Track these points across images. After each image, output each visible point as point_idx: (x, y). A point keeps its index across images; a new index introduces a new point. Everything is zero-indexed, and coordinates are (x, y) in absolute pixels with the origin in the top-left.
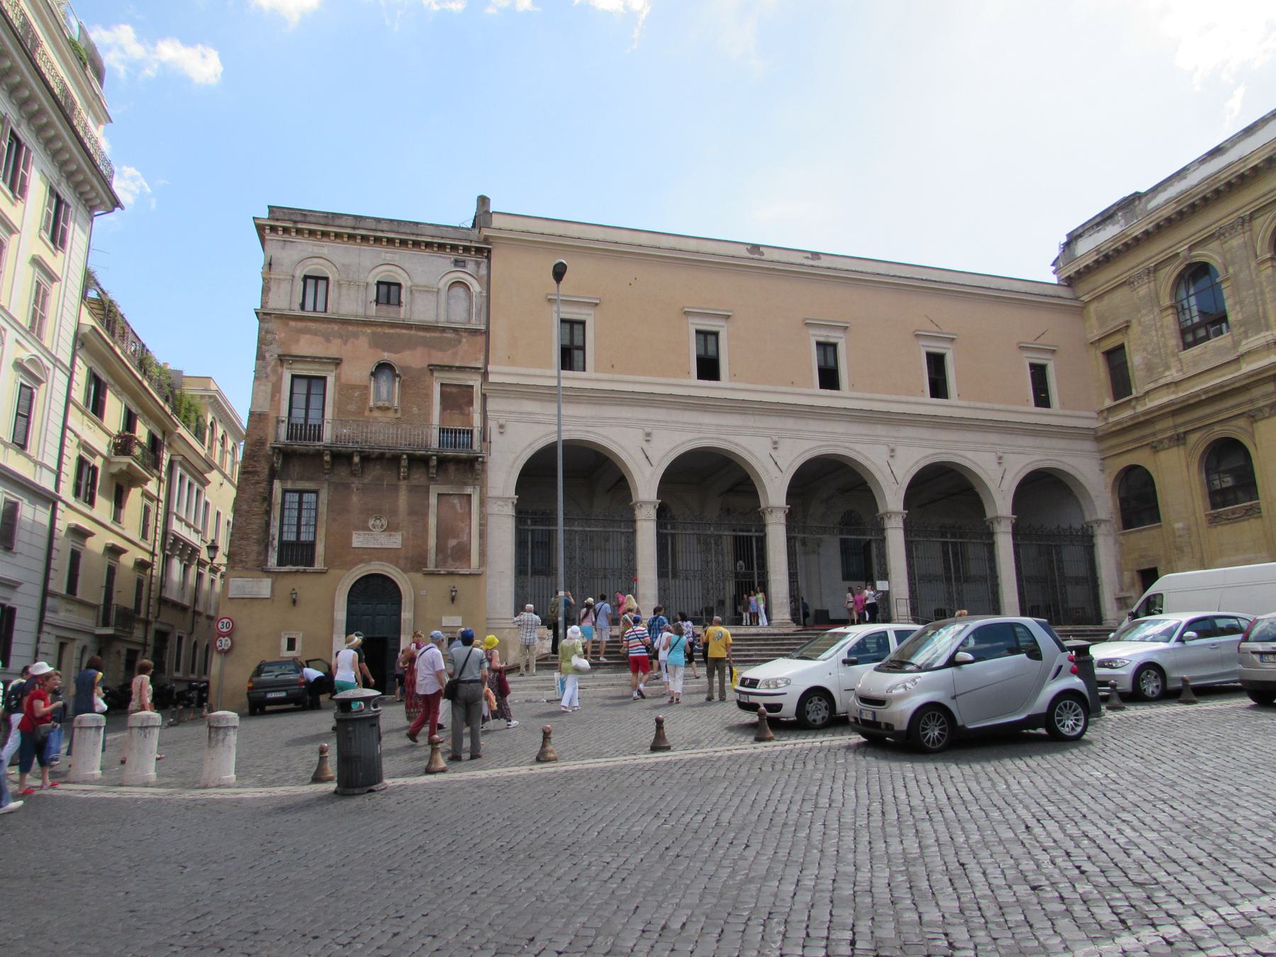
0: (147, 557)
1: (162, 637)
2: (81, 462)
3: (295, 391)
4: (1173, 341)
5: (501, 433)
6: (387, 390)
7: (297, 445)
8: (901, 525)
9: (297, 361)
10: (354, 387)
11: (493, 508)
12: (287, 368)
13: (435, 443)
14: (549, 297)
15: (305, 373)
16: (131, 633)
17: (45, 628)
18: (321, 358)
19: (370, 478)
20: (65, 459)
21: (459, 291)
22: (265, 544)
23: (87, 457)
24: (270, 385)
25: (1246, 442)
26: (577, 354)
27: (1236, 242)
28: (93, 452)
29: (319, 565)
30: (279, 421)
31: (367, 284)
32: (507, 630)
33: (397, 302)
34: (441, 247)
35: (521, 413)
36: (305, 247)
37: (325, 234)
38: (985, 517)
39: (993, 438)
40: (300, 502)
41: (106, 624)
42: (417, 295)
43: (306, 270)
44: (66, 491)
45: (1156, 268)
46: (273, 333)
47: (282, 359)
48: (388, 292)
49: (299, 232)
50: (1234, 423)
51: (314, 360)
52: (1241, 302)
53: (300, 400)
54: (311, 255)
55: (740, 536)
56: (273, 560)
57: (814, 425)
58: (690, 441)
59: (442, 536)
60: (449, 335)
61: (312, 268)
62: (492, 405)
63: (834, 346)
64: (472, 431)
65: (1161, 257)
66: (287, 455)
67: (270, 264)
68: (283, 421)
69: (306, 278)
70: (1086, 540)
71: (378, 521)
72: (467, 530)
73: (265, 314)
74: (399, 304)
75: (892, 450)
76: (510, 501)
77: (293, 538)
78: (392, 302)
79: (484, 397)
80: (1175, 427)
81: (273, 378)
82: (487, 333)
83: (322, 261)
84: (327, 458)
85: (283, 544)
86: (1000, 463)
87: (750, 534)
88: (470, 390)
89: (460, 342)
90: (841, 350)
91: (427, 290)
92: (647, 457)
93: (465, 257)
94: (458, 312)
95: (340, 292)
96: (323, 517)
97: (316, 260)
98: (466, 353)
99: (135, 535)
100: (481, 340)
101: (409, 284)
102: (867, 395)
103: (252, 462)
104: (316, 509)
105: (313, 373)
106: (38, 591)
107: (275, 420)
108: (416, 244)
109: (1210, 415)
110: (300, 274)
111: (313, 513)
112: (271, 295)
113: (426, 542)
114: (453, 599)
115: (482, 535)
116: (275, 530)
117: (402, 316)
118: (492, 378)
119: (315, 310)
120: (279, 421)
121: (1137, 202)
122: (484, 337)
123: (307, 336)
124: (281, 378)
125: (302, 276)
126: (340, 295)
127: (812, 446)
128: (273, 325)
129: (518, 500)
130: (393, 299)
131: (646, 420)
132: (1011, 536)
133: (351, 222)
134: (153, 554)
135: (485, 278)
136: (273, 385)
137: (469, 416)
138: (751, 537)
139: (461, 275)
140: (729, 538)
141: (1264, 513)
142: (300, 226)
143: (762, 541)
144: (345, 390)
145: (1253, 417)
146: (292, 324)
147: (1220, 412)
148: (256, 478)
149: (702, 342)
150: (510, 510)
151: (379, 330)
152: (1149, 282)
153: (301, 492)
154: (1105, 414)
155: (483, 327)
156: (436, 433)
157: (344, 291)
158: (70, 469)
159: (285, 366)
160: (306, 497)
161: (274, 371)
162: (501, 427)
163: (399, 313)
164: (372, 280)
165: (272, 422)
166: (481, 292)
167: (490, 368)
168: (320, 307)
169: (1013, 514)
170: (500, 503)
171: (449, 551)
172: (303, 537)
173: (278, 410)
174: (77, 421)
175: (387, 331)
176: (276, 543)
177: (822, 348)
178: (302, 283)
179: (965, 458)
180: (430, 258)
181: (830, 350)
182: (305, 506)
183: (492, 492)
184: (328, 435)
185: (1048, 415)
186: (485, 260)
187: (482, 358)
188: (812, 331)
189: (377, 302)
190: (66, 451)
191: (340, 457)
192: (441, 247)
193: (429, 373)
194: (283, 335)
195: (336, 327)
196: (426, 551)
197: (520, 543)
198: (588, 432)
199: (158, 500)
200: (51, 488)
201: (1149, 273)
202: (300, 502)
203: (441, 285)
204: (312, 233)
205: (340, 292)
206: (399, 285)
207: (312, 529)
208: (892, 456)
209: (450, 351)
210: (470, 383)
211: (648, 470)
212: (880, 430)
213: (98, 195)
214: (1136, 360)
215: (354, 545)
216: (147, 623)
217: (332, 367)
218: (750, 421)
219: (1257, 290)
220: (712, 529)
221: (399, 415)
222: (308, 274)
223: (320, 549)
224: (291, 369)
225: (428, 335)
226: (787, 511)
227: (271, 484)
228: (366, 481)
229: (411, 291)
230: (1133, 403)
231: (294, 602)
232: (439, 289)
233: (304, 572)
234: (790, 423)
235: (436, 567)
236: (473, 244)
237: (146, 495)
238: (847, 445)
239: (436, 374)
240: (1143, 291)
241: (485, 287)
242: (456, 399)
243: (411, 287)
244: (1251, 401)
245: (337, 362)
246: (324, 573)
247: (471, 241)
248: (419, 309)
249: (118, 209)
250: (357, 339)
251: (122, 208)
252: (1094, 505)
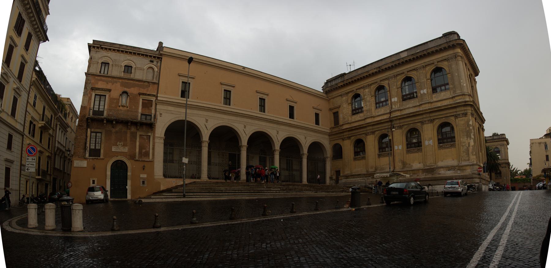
0: (50, 155)
1: (55, 179)
2: (31, 123)
3: (96, 100)
4: (350, 112)
5: (161, 116)
6: (124, 100)
7: (96, 117)
8: (279, 154)
9: (97, 90)
10: (114, 99)
11: (157, 140)
12: (94, 92)
13: (139, 119)
14: (179, 74)
15: (99, 94)
16: (46, 178)
17: (22, 176)
18: (105, 89)
19: (118, 129)
20: (26, 121)
21: (151, 70)
22: (85, 149)
23: (32, 121)
24: (88, 97)
25: (364, 141)
26: (186, 93)
27: (367, 90)
28: (35, 120)
29: (102, 157)
30: (90, 109)
31: (121, 66)
33: (130, 72)
34: (147, 56)
36: (103, 53)
37: (110, 49)
38: (300, 153)
39: (304, 132)
40: (96, 136)
41: (39, 175)
42: (137, 70)
43: (103, 60)
44: (26, 132)
45: (348, 93)
46: (90, 80)
47: (93, 89)
48: (128, 68)
49: (102, 48)
50: (362, 135)
51: (102, 90)
52: (367, 105)
53: (97, 103)
54: (105, 56)
56: (87, 155)
59: (141, 148)
60: (146, 84)
61: (103, 60)
62: (158, 107)
63: (264, 100)
64: (151, 115)
65: (349, 90)
66: (93, 120)
67: (91, 58)
68: (91, 109)
69: (102, 63)
70: (324, 161)
71: (120, 143)
72: (148, 147)
73: (88, 74)
74: (131, 73)
75: (278, 132)
76: (163, 138)
77: (93, 148)
78: (129, 72)
79: (156, 104)
80: (349, 134)
81: (89, 95)
82: (158, 84)
83: (108, 58)
84: (105, 122)
85: (90, 150)
86: (305, 139)
87: (236, 153)
88: (151, 102)
89: (149, 86)
90: (266, 101)
91: (141, 69)
92: (206, 127)
93: (153, 59)
94: (149, 77)
95: (112, 68)
96: (103, 141)
97: (106, 57)
98: (151, 90)
99: (47, 148)
100: (156, 86)
101: (135, 67)
103: (81, 123)
104: (101, 138)
105: (102, 94)
106: (19, 164)
107: (89, 109)
108: (139, 54)
109: (357, 133)
110: (100, 61)
111: (100, 140)
112: (90, 68)
113: (135, 150)
114: (144, 169)
115: (153, 149)
116: (88, 145)
117: (131, 77)
118: (159, 98)
119: (104, 73)
120: (90, 109)
121: (345, 76)
122: (157, 85)
123: (101, 82)
124: (91, 95)
125: (101, 62)
126: (112, 70)
128: (90, 78)
129: (165, 138)
130: (129, 71)
131: (207, 116)
132: (306, 159)
133: (118, 46)
134: (51, 153)
135: (159, 67)
136: (89, 98)
137: (151, 110)
138: (236, 154)
139: (152, 65)
141: (366, 159)
142: (102, 46)
143: (239, 156)
144: (111, 100)
145: (367, 134)
146: (97, 77)
147: (359, 132)
148: (82, 128)
149: (226, 93)
150: (162, 141)
151: (124, 81)
152: (346, 96)
153: (96, 133)
154: (332, 129)
155: (157, 82)
156: (140, 115)
157: (114, 68)
158: (27, 125)
159: (93, 91)
160: (98, 134)
161: (90, 93)
162: (161, 114)
163: (130, 76)
164: (123, 64)
165: (88, 110)
166: (157, 71)
167: (158, 95)
168: (106, 72)
169: (308, 153)
170: (159, 139)
171: (143, 153)
172: (97, 148)
173: (90, 105)
174: (30, 109)
175: (126, 81)
176: (88, 149)
177: (260, 100)
178: (101, 65)
179: (297, 136)
180: (142, 59)
181: (263, 100)
182: (97, 137)
183: (156, 135)
184: (105, 114)
185: (318, 127)
186: (160, 61)
187: (156, 92)
188: (258, 94)
189: (124, 72)
190: (26, 119)
191: (110, 121)
192: (147, 56)
193: (139, 95)
194: (93, 81)
195: (110, 79)
196: (136, 153)
197: (165, 153)
199: (53, 137)
200: (22, 130)
201: (346, 94)
202: (96, 136)
203: (145, 68)
204: (106, 49)
205: (112, 68)
206: (131, 67)
207: (99, 145)
208: (278, 134)
209: (146, 89)
210: (152, 100)
211: (206, 131)
213: (42, 36)
214: (341, 116)
215: (113, 151)
216: (50, 175)
217: (108, 92)
219: (370, 103)
221: (128, 109)
223: (102, 151)
224: (95, 92)
225: (139, 83)
227: (87, 130)
228: (117, 130)
229: (135, 69)
230: (339, 127)
231: (94, 168)
232: (144, 69)
233: (97, 159)
235: (139, 158)
236: (157, 56)
237: (50, 134)
238: (266, 129)
239: (141, 96)
240: (344, 98)
241: (159, 69)
242: (147, 104)
243: (135, 68)
244: (367, 130)
245: (110, 91)
246: (103, 159)
247: (156, 55)
248: (138, 75)
249: (47, 41)
250: (117, 83)
251: (49, 41)
252: (327, 153)
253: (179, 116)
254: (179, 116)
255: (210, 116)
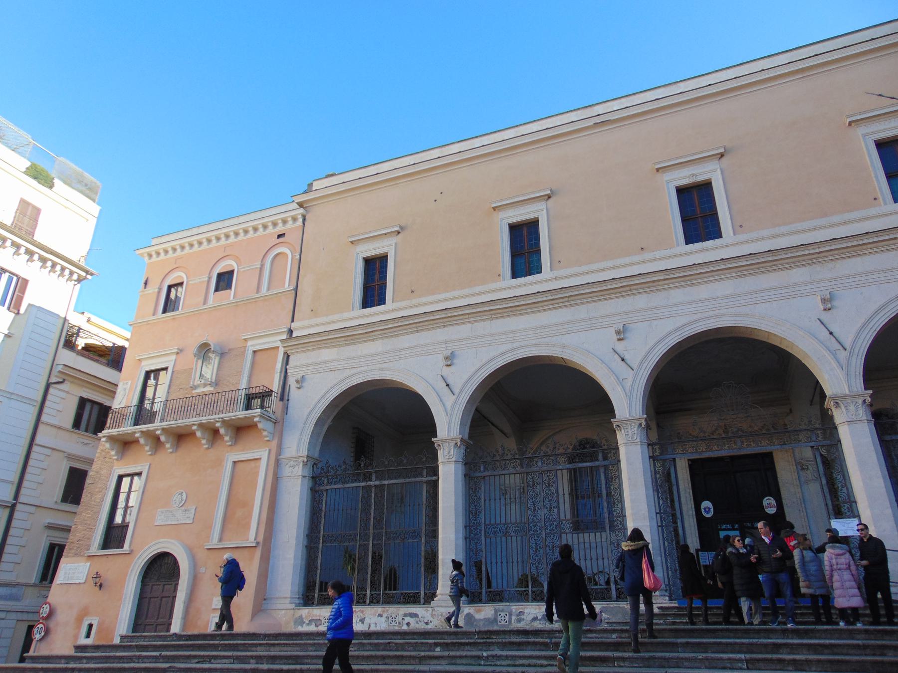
32: (283, 612)
35: (317, 364)
55: (580, 468)
57: (677, 295)
58: (502, 354)
102: (766, 233)
118: (294, 335)
127: (678, 324)
131: (446, 342)
140: (565, 472)
162: (297, 382)
198: (383, 369)
211: (449, 400)
212: (798, 274)
218: (582, 311)
220: (540, 464)
222: (170, 284)
226: (644, 423)
234: (640, 301)
253: (354, 371)
254: (354, 371)
255: (460, 340)
